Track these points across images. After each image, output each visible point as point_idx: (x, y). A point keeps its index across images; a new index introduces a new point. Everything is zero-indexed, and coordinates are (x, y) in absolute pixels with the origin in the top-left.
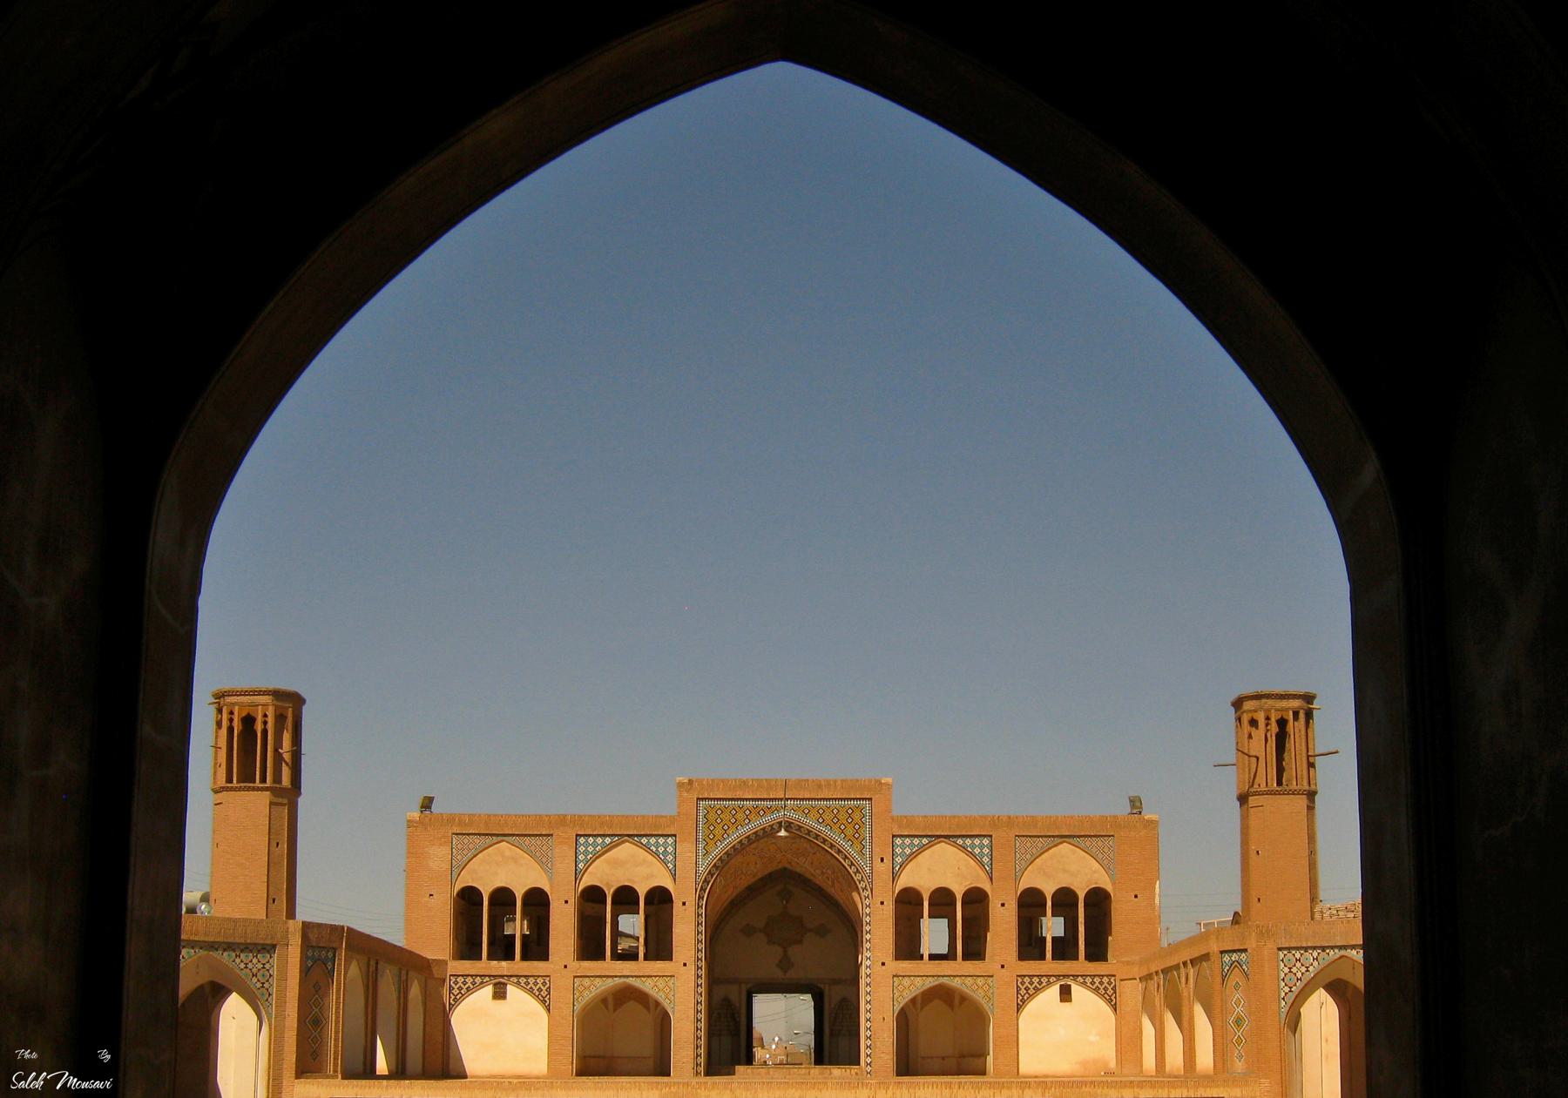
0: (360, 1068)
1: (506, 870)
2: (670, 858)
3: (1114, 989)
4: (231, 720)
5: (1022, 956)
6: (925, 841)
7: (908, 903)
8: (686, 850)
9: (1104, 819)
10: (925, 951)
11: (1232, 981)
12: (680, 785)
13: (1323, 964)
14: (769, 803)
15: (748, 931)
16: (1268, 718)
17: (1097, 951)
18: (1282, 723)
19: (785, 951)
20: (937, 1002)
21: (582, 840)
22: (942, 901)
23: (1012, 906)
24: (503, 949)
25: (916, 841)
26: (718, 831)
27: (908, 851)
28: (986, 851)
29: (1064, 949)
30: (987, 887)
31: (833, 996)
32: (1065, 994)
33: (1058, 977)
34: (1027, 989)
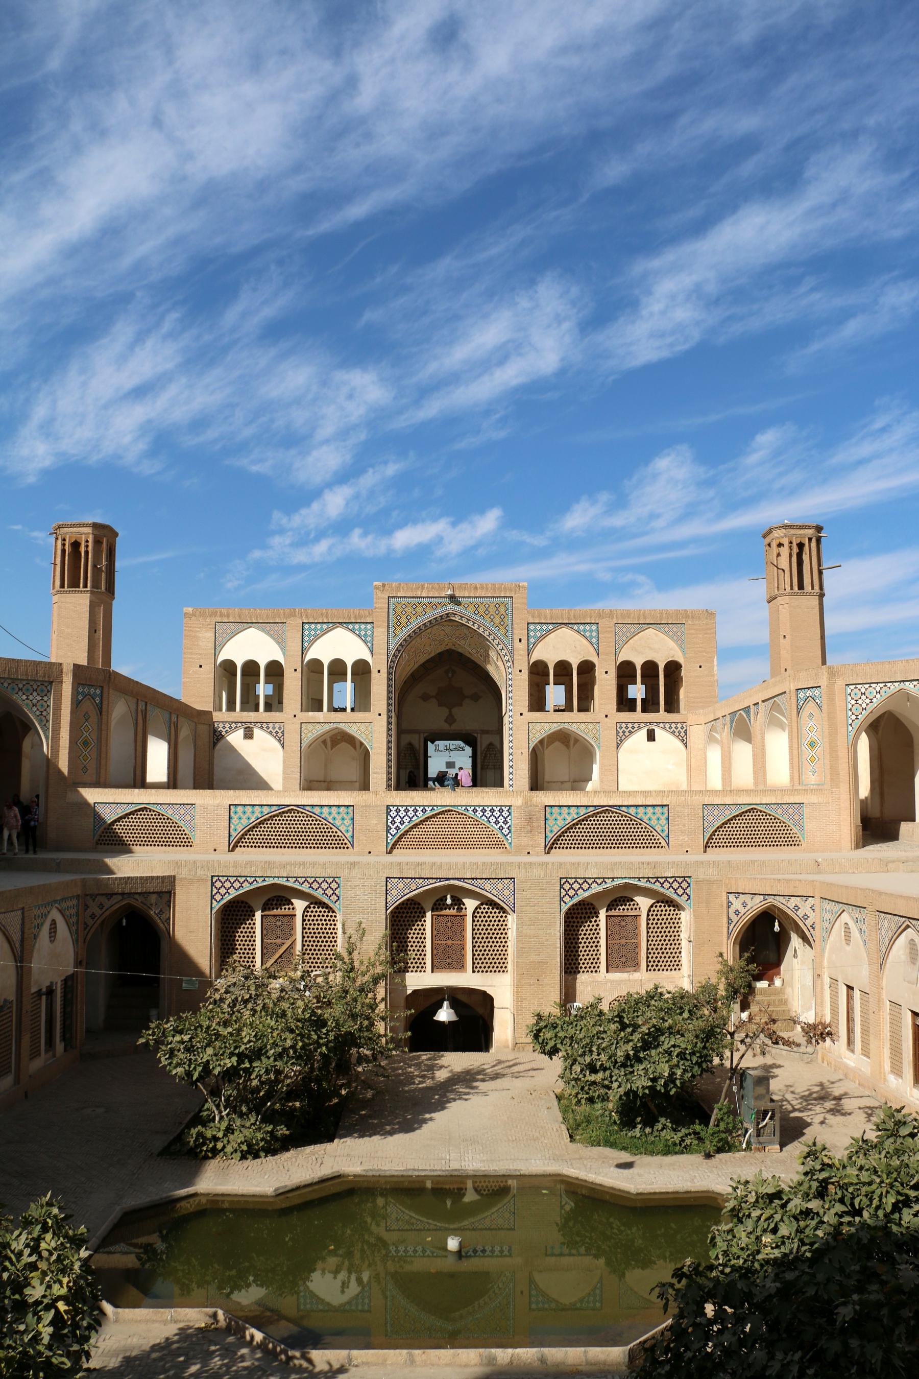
0: (132, 783)
1: (252, 646)
2: (369, 639)
3: (685, 732)
4: (64, 545)
5: (620, 709)
6: (551, 627)
7: (538, 672)
8: (380, 634)
9: (677, 612)
10: (550, 705)
11: (805, 713)
12: (377, 588)
13: (885, 696)
14: (440, 600)
15: (425, 697)
16: (791, 543)
17: (672, 705)
18: (801, 546)
19: (450, 712)
20: (557, 744)
21: (306, 626)
22: (563, 668)
23: (613, 673)
24: (250, 703)
25: (544, 627)
26: (404, 620)
27: (539, 634)
28: (594, 634)
29: (649, 705)
30: (594, 659)
31: (483, 742)
32: (651, 737)
33: (646, 724)
34: (624, 732)
